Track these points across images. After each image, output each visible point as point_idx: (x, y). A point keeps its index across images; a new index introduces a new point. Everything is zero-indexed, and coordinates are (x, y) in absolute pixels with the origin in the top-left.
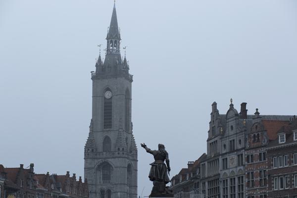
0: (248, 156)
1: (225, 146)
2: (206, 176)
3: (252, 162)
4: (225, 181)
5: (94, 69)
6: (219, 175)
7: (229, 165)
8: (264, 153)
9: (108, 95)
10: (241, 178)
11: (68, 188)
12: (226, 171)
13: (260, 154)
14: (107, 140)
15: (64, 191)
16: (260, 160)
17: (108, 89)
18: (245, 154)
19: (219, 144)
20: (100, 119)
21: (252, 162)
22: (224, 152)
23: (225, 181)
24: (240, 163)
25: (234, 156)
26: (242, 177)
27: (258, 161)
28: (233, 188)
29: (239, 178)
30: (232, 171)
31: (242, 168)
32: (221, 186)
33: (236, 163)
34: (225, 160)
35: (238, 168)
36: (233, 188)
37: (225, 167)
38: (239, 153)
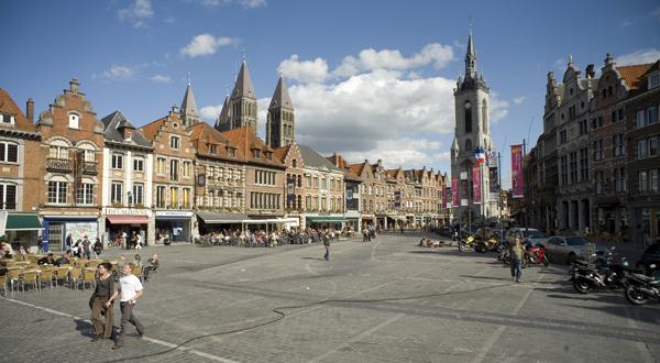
0: (594, 121)
1: (563, 116)
2: (543, 155)
3: (601, 125)
4: (564, 158)
5: (456, 87)
6: (556, 151)
7: (569, 137)
8: (620, 111)
9: (468, 106)
10: (584, 151)
11: (423, 180)
12: (566, 146)
13: (614, 114)
14: (468, 142)
15: (420, 182)
16: (614, 121)
17: (467, 101)
18: (589, 118)
19: (557, 115)
20: (463, 126)
21: (601, 125)
22: (562, 122)
23: (564, 158)
24: (583, 130)
25: (576, 126)
26: (586, 149)
27: (611, 123)
28: (574, 165)
29: (582, 151)
30: (574, 145)
31: (586, 137)
32: (559, 163)
33: (577, 132)
34: (563, 133)
35: (580, 139)
36: (574, 165)
37: (564, 140)
38: (582, 119)
